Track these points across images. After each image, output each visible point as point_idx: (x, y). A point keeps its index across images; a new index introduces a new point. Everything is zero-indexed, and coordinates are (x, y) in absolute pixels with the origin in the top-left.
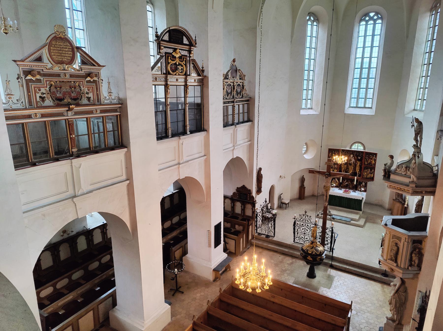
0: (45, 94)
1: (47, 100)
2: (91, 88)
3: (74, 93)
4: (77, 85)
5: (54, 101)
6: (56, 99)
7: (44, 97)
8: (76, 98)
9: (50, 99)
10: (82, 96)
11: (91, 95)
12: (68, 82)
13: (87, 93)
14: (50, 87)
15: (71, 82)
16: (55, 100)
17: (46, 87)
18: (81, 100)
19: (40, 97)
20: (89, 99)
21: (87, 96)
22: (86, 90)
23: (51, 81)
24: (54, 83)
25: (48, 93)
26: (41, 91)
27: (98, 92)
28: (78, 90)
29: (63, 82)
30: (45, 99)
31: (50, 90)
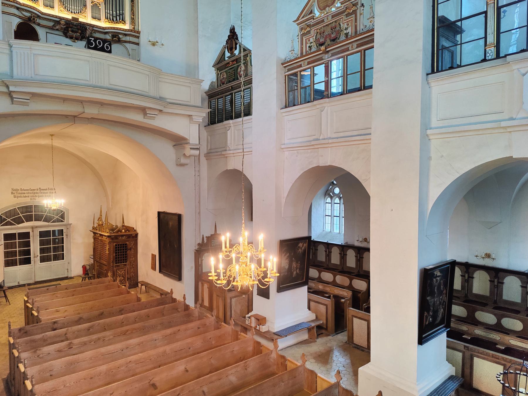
0: (312, 42)
1: (313, 48)
2: (351, 21)
3: (334, 33)
4: (338, 24)
5: (318, 47)
6: (319, 45)
7: (312, 46)
8: (335, 38)
9: (315, 46)
10: (340, 34)
11: (349, 30)
12: (330, 24)
13: (346, 29)
14: (316, 36)
15: (332, 23)
16: (318, 46)
17: (314, 36)
18: (339, 39)
19: (309, 47)
20: (347, 35)
21: (345, 32)
22: (346, 26)
23: (317, 29)
24: (320, 30)
25: (314, 42)
26: (310, 41)
27: (356, 24)
28: (338, 28)
29: (326, 25)
30: (312, 47)
31: (316, 39)
